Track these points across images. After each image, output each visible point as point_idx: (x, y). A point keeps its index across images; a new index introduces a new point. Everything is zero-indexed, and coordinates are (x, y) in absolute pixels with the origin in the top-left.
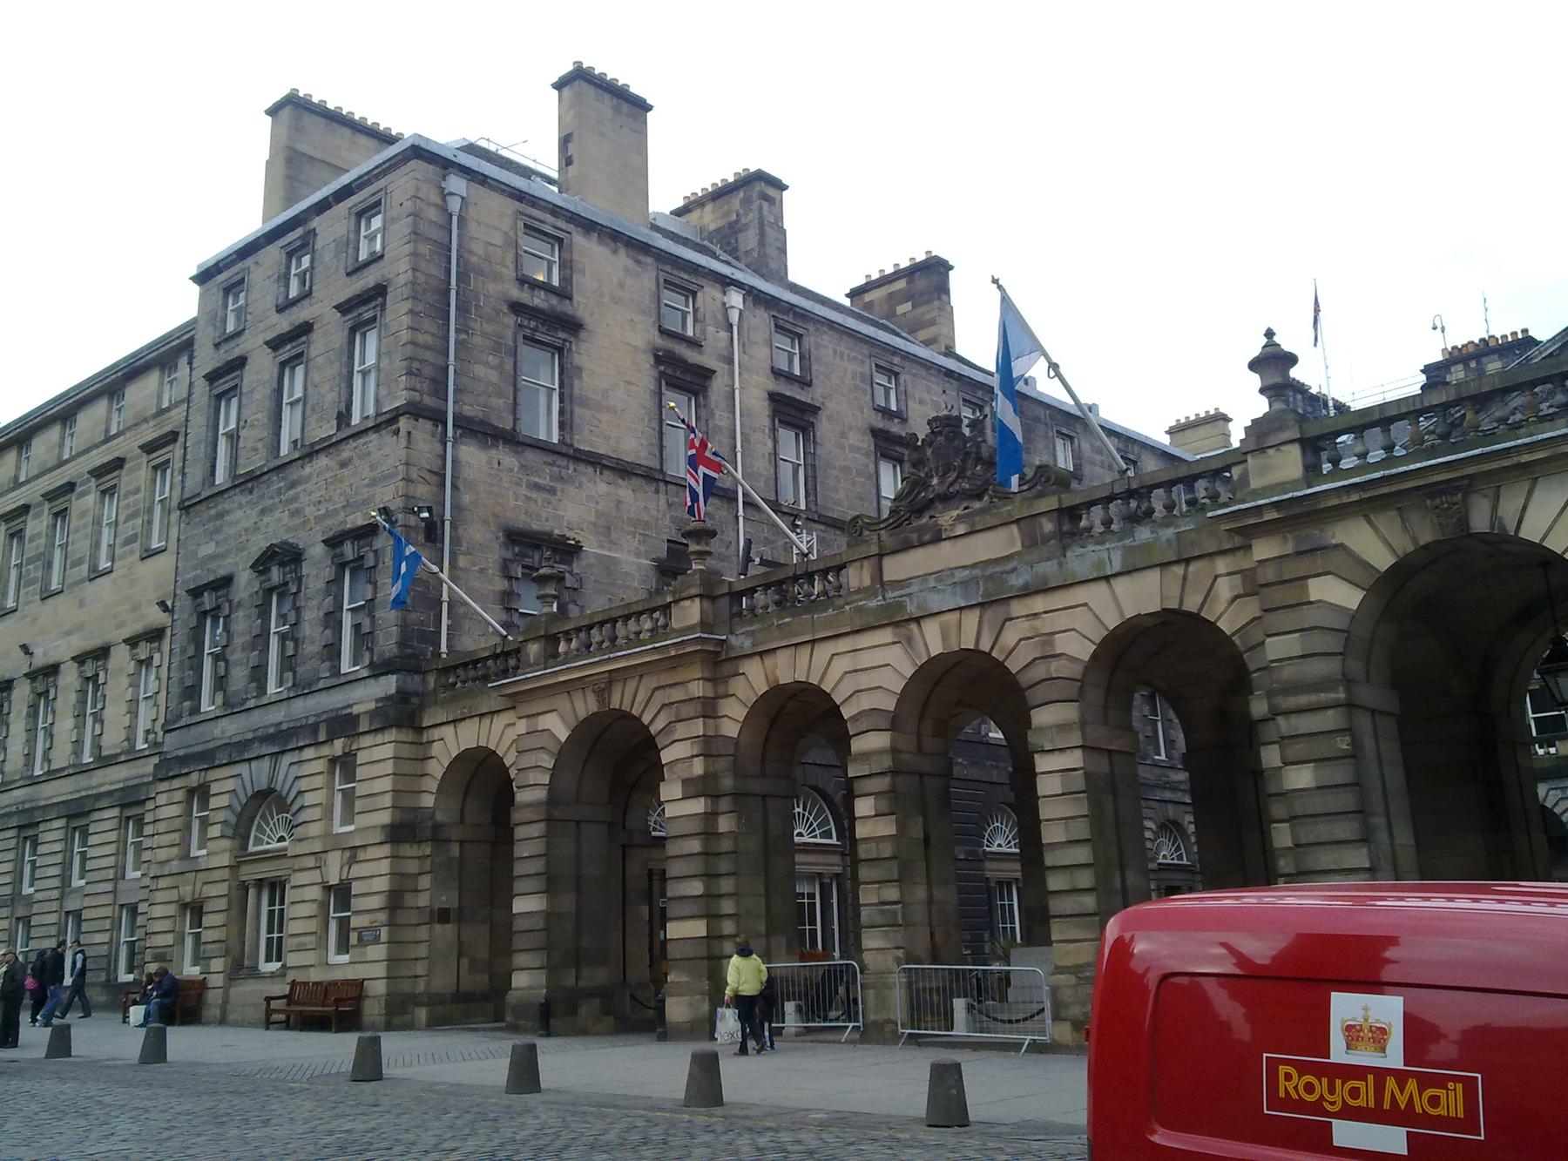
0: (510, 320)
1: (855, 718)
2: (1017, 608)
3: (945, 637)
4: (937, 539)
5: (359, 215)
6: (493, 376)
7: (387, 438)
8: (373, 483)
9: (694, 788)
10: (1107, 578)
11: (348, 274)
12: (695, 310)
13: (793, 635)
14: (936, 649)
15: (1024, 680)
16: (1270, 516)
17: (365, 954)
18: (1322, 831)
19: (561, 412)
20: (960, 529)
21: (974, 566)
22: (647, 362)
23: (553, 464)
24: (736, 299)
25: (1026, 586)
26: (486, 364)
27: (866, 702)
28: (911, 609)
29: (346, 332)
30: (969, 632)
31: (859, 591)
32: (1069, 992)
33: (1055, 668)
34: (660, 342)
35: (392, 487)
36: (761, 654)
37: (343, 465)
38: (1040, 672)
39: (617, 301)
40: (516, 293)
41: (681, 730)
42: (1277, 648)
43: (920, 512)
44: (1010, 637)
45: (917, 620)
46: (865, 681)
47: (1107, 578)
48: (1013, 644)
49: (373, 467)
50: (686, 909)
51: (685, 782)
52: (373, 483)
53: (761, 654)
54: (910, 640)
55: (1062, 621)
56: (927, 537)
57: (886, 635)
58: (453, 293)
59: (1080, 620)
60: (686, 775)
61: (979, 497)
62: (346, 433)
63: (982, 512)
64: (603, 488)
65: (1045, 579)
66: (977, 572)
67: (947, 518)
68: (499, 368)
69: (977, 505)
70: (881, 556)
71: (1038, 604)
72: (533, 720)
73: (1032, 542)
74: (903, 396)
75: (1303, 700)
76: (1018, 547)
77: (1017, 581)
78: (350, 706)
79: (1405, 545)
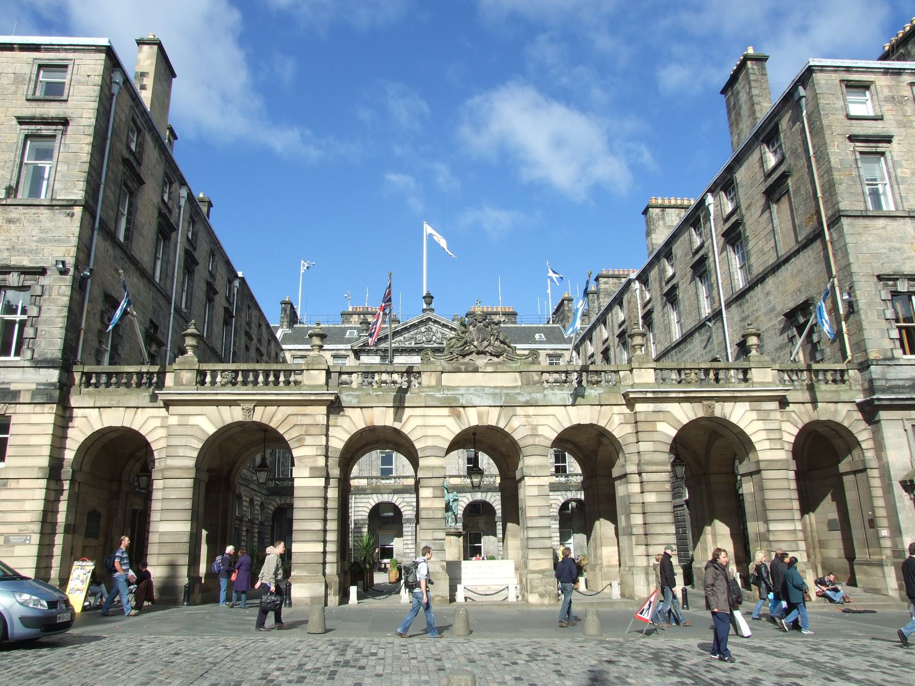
0: (121, 167)
1: (423, 449)
2: (519, 410)
3: (480, 416)
4: (476, 370)
5: (40, 67)
6: (112, 199)
7: (60, 217)
8: (42, 241)
9: (314, 472)
10: (565, 406)
11: (27, 100)
12: (170, 193)
13: (384, 402)
14: (474, 422)
15: (521, 444)
16: (650, 395)
17: (13, 551)
18: (658, 519)
19: (127, 230)
20: (490, 369)
21: (495, 387)
22: (156, 215)
23: (122, 259)
24: (184, 193)
25: (527, 402)
26: (111, 189)
27: (430, 442)
28: (463, 401)
29: (22, 137)
30: (493, 418)
31: (428, 387)
32: (539, 581)
33: (537, 440)
34: (162, 206)
35: (64, 249)
36: (361, 408)
37: (10, 221)
38: (530, 441)
39: (152, 175)
40: (127, 155)
41: (309, 440)
42: (643, 446)
43: (464, 356)
44: (516, 423)
45: (464, 407)
46: (430, 432)
47: (565, 406)
48: (517, 426)
49: (42, 231)
50: (308, 537)
51: (312, 469)
52: (42, 241)
53: (361, 408)
54: (459, 416)
55: (542, 421)
56: (470, 369)
57: (446, 411)
58: (108, 141)
59: (551, 421)
60: (313, 465)
61: (498, 356)
62: (9, 201)
63: (499, 363)
64: (136, 280)
65: (536, 401)
66: (497, 391)
67: (481, 361)
68: (114, 193)
69: (495, 359)
70: (442, 372)
71: (531, 411)
72: (184, 418)
73: (527, 383)
74: (215, 267)
75: (654, 468)
76: (519, 384)
77: (522, 399)
78: (9, 383)
79: (693, 417)
